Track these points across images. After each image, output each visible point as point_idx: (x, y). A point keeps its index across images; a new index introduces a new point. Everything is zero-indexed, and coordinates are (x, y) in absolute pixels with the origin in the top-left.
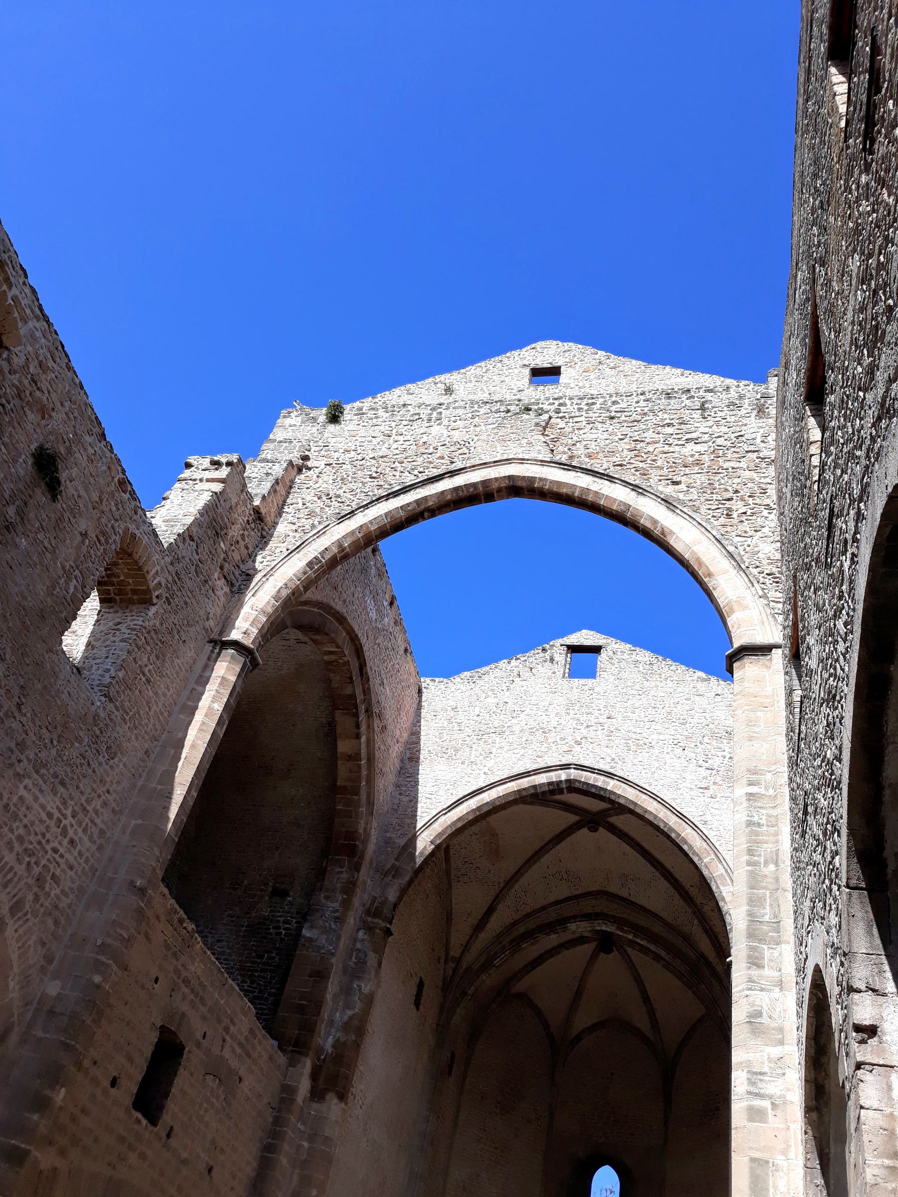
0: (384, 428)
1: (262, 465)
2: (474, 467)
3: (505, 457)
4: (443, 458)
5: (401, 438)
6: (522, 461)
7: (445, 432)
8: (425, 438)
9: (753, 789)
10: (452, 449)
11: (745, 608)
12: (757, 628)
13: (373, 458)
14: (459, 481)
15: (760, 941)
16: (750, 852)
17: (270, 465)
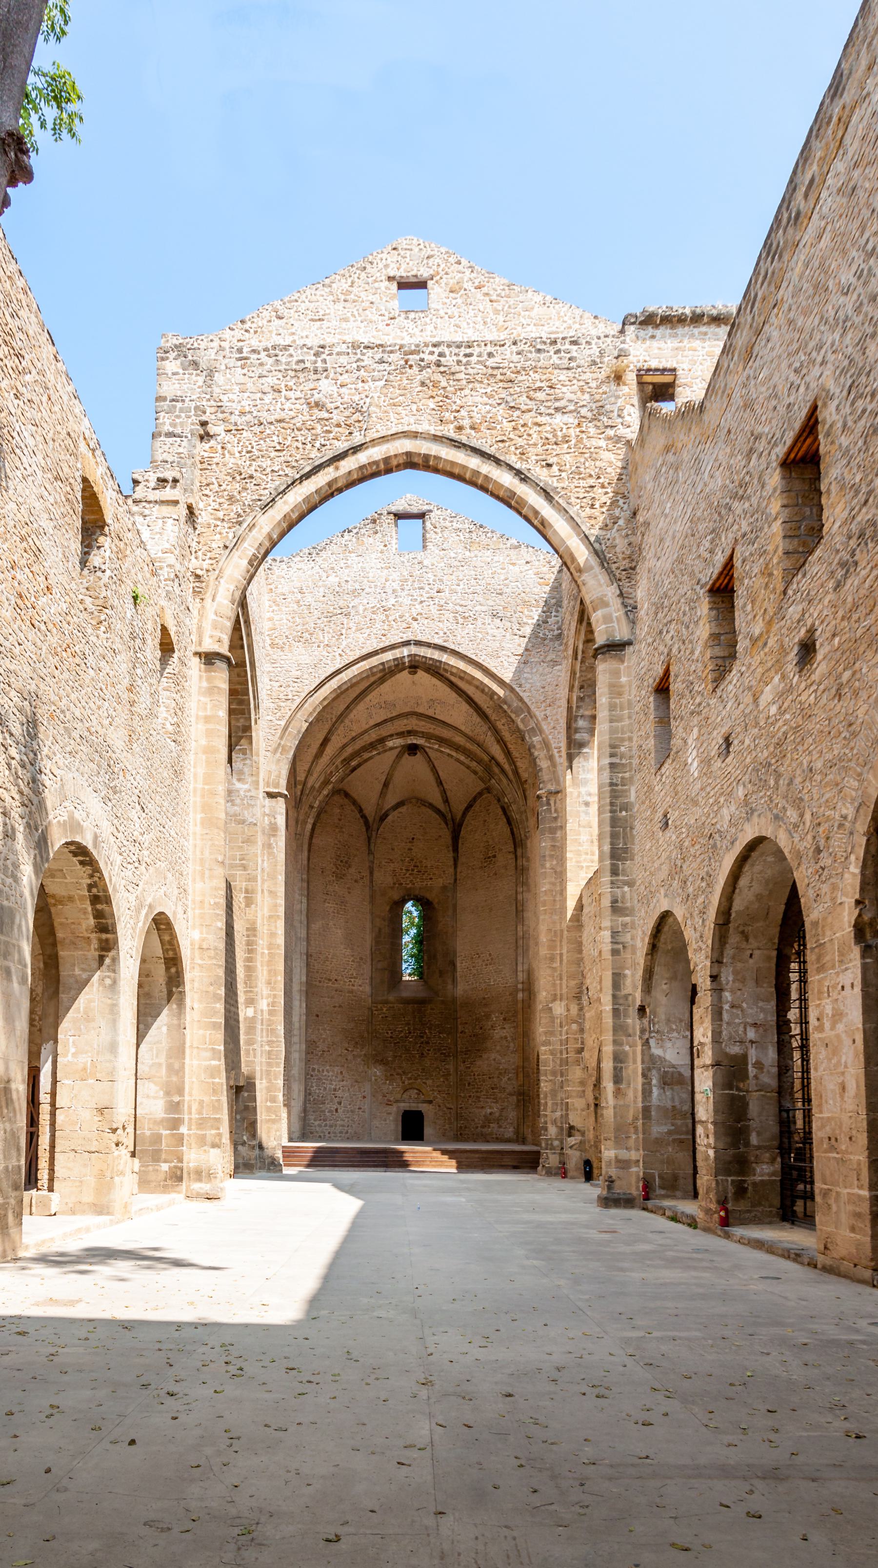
0: (271, 380)
1: (171, 440)
2: (374, 442)
3: (400, 429)
4: (338, 425)
5: (291, 394)
6: (415, 435)
7: (335, 388)
8: (317, 397)
9: (615, 760)
10: (347, 413)
11: (606, 605)
12: (615, 625)
13: (271, 423)
14: (363, 458)
15: (618, 860)
16: (612, 804)
17: (178, 439)
